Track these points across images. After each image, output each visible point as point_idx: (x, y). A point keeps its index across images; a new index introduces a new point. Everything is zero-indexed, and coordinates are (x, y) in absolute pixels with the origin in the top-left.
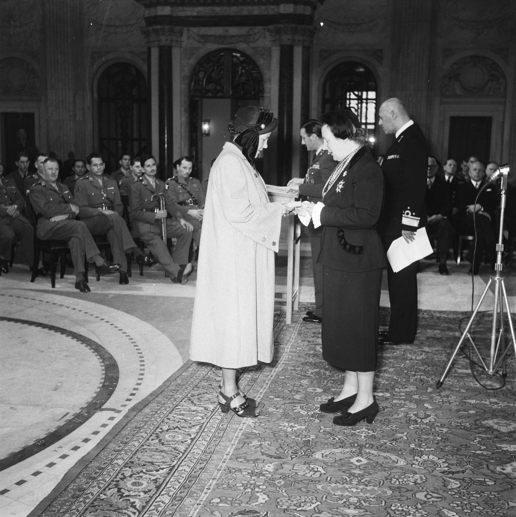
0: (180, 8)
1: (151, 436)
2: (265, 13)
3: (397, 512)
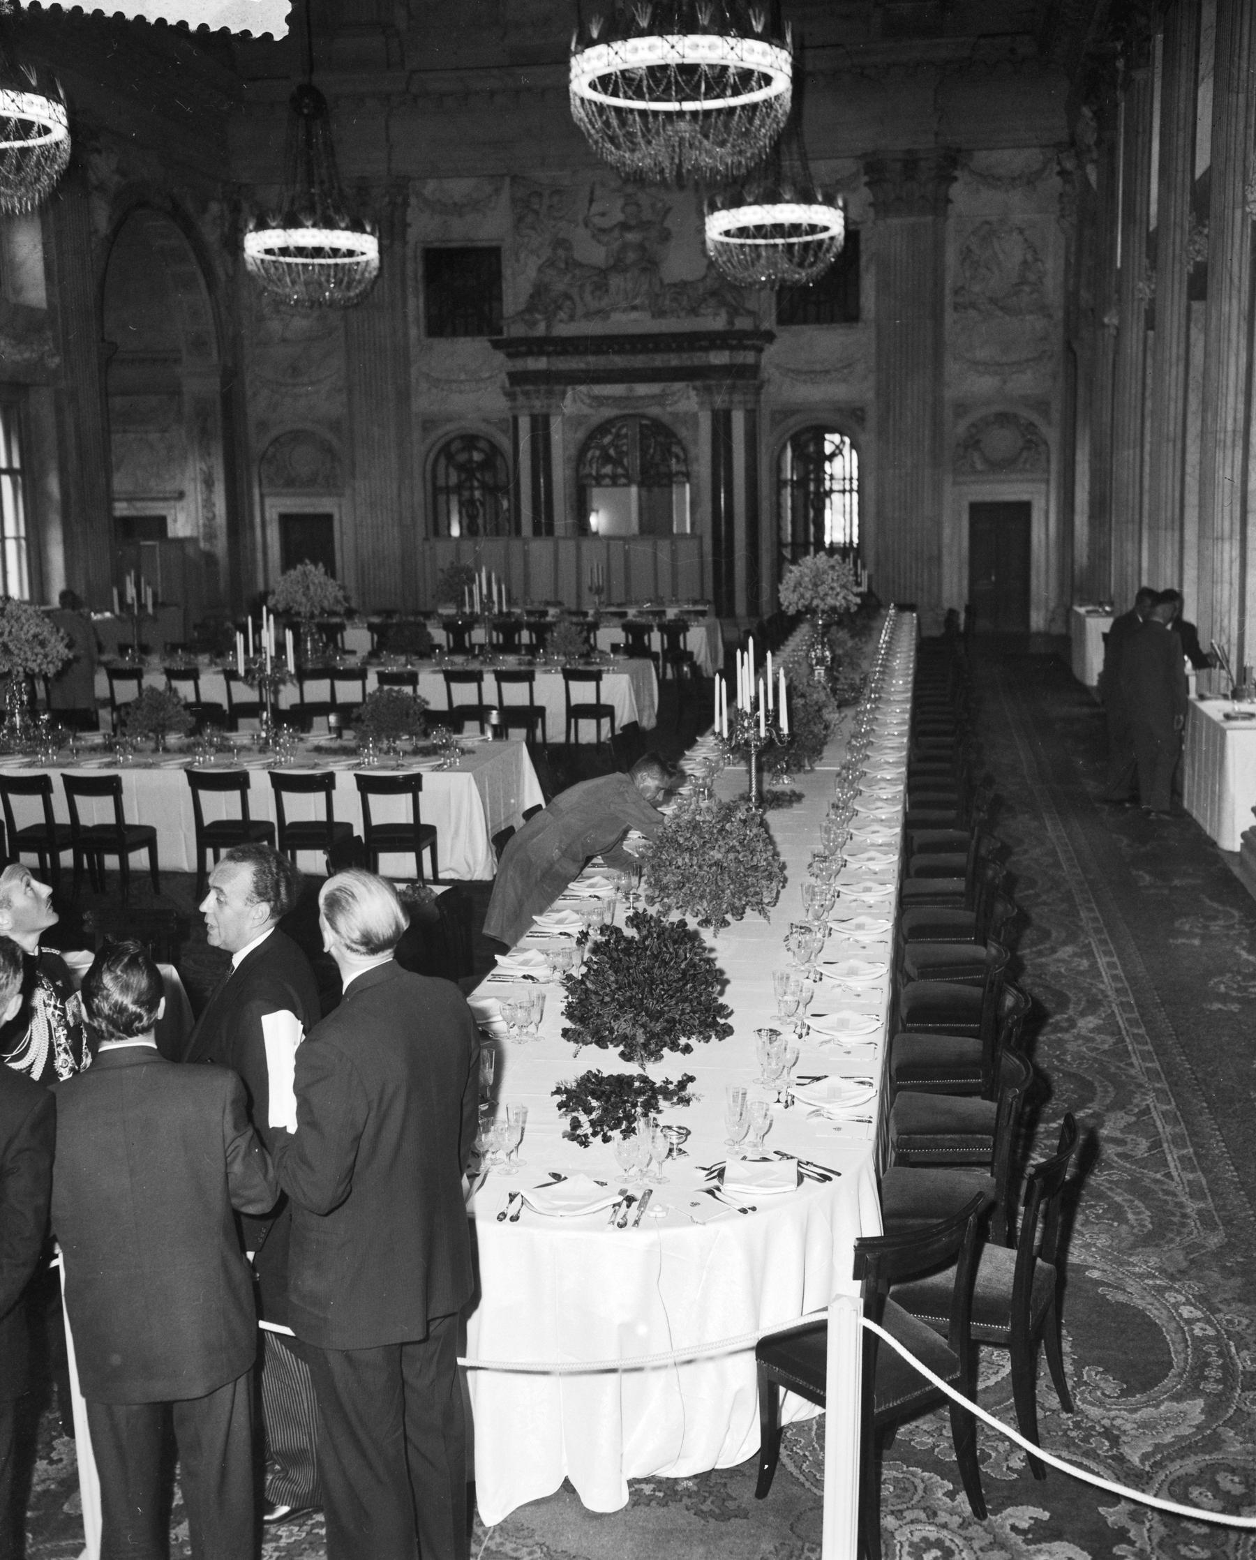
2: (689, 363)
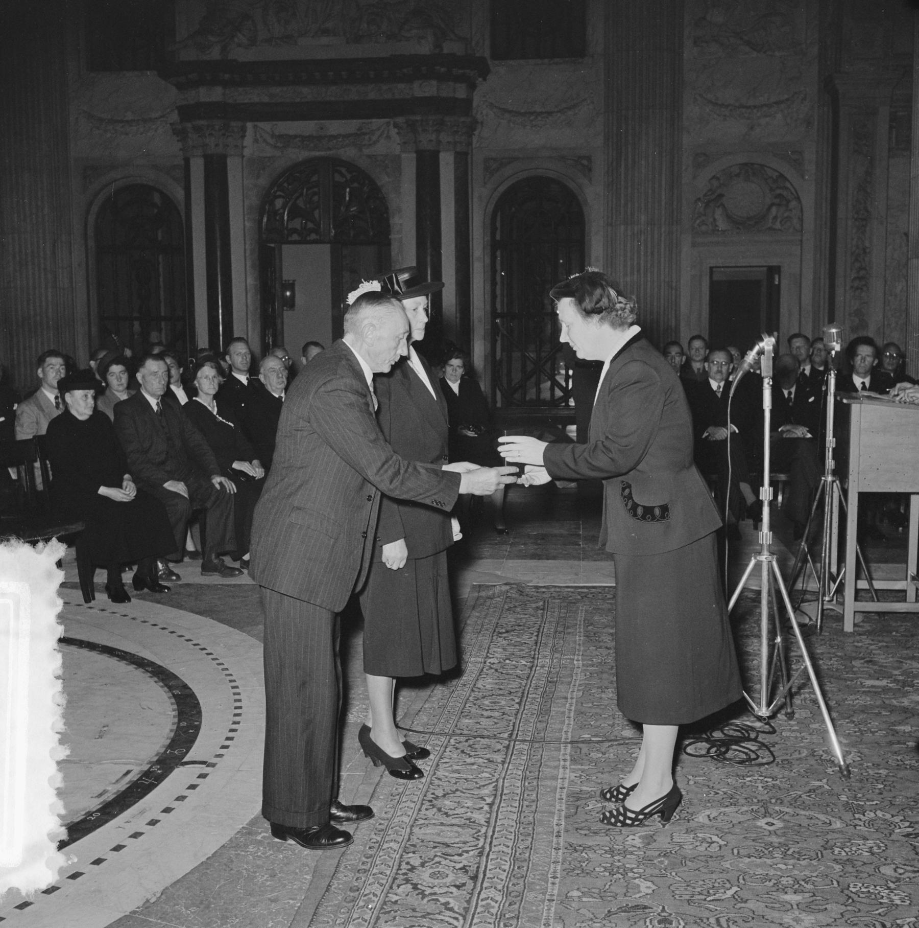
0: (241, 89)
1: (422, 804)
3: (861, 895)
